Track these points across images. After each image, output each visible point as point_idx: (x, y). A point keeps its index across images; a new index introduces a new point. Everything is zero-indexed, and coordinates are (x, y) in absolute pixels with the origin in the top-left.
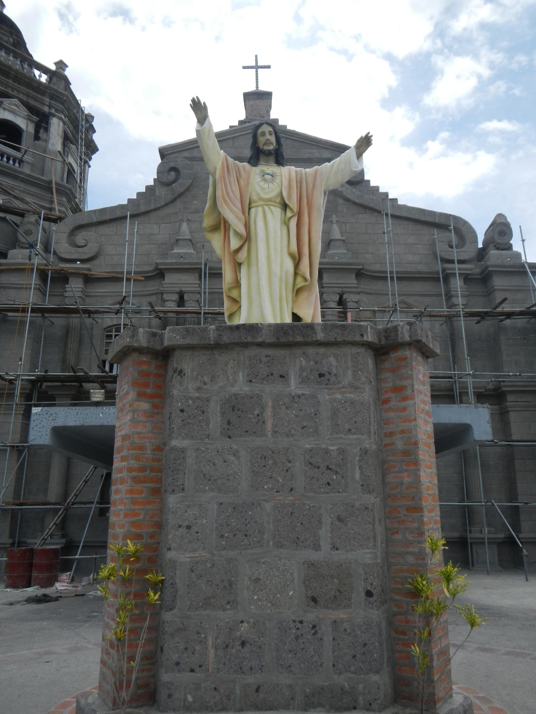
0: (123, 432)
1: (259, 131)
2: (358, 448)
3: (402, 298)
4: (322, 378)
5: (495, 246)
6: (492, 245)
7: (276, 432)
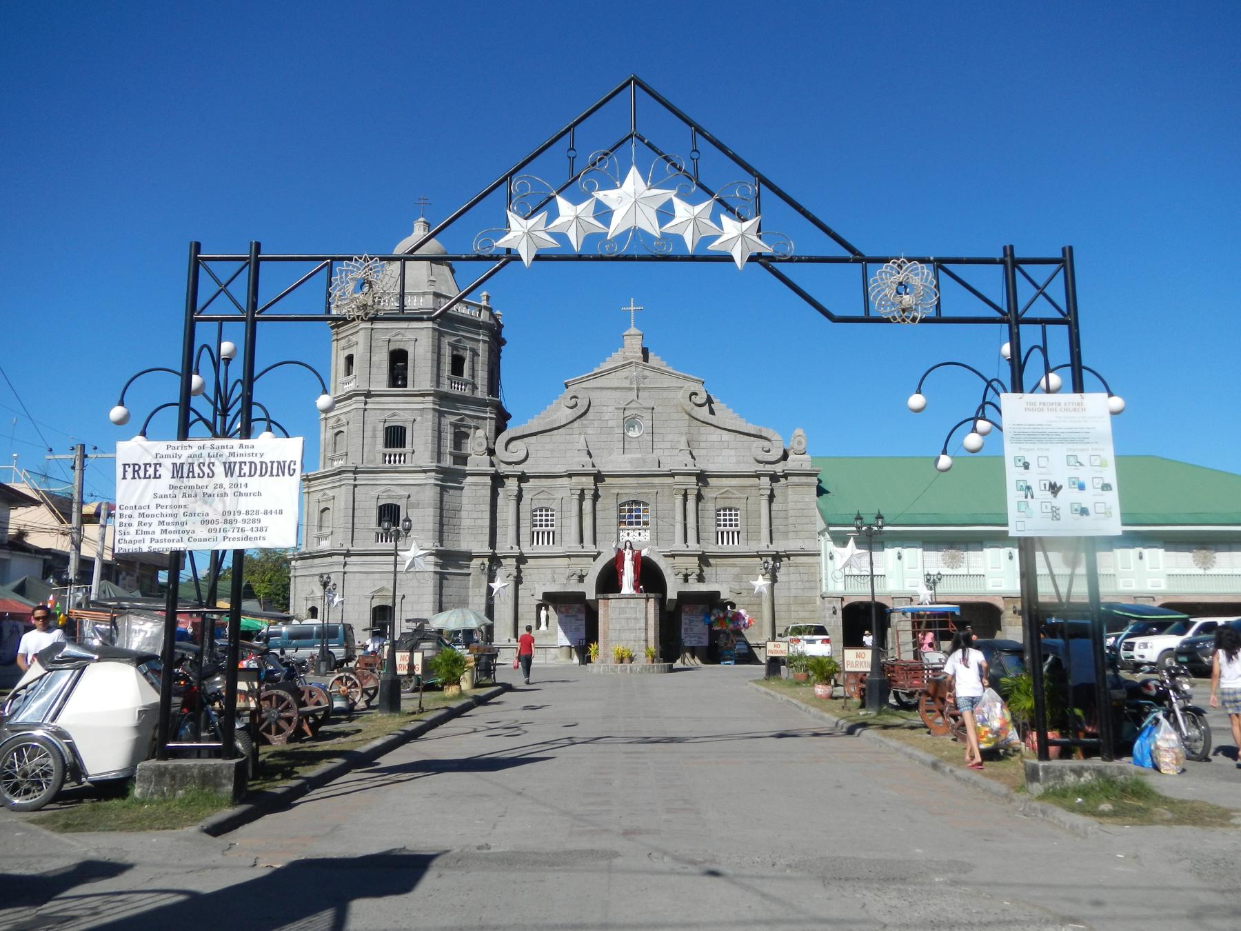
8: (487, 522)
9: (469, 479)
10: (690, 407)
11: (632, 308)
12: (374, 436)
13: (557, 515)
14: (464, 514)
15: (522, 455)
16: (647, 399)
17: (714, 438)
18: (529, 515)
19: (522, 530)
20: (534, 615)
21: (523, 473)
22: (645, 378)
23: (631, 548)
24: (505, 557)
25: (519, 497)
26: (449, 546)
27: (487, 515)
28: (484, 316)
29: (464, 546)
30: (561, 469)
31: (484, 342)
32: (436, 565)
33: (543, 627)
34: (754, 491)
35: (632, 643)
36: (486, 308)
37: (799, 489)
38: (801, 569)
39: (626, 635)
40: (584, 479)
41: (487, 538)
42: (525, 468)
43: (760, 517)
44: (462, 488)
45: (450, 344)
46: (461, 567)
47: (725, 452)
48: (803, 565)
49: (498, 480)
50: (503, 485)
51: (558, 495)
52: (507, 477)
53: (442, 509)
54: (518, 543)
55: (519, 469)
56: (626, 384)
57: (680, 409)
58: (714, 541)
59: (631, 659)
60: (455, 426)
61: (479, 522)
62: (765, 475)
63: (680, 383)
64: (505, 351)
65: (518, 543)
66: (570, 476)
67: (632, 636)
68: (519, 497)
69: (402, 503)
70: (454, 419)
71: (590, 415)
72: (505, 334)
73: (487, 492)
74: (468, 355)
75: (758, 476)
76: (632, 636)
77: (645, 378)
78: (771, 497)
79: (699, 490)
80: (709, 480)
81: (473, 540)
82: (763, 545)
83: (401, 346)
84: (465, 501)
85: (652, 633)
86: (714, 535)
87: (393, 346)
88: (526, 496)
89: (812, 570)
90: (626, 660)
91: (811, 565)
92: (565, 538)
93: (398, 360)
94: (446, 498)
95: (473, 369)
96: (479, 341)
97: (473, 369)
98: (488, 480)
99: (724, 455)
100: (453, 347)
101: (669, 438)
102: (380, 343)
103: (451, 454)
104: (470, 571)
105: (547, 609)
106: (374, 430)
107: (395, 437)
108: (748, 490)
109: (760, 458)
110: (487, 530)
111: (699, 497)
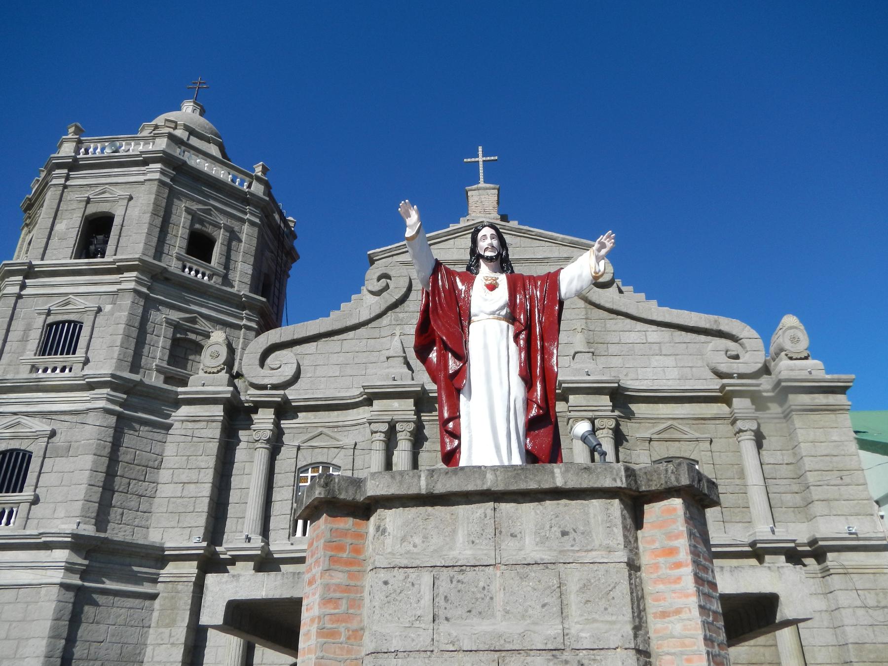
1: (480, 234)
2: (619, 636)
3: (670, 423)
4: (566, 537)
5: (786, 355)
6: (783, 353)
7: (507, 612)
8: (206, 490)
9: (185, 411)
11: (481, 159)
12: (24, 340)
14: (164, 475)
15: (288, 372)
17: (633, 337)
21: (286, 401)
23: (502, 262)
25: (275, 444)
26: (117, 533)
28: (257, 189)
29: (154, 537)
30: (354, 392)
31: (252, 224)
32: (70, 568)
34: (724, 429)
36: (258, 179)
38: (859, 581)
40: (395, 404)
41: (201, 520)
42: (292, 394)
43: (742, 474)
44: (168, 427)
45: (188, 211)
47: (656, 361)
48: (861, 570)
49: (237, 415)
50: (248, 424)
51: (347, 440)
52: (256, 407)
53: (113, 459)
54: (265, 532)
55: (276, 396)
60: (176, 327)
61: (191, 489)
62: (740, 394)
65: (265, 532)
66: (369, 400)
68: (275, 444)
69: (36, 448)
70: (175, 316)
72: (297, 244)
74: (221, 237)
75: (725, 398)
79: (618, 425)
80: (634, 407)
81: (172, 520)
82: (762, 530)
83: (103, 208)
84: (170, 450)
87: (92, 209)
93: (96, 231)
94: (129, 439)
95: (228, 257)
96: (243, 221)
97: (228, 257)
98: (218, 411)
102: (75, 205)
103: (159, 370)
106: (28, 329)
107: (60, 337)
108: (711, 426)
110: (204, 505)
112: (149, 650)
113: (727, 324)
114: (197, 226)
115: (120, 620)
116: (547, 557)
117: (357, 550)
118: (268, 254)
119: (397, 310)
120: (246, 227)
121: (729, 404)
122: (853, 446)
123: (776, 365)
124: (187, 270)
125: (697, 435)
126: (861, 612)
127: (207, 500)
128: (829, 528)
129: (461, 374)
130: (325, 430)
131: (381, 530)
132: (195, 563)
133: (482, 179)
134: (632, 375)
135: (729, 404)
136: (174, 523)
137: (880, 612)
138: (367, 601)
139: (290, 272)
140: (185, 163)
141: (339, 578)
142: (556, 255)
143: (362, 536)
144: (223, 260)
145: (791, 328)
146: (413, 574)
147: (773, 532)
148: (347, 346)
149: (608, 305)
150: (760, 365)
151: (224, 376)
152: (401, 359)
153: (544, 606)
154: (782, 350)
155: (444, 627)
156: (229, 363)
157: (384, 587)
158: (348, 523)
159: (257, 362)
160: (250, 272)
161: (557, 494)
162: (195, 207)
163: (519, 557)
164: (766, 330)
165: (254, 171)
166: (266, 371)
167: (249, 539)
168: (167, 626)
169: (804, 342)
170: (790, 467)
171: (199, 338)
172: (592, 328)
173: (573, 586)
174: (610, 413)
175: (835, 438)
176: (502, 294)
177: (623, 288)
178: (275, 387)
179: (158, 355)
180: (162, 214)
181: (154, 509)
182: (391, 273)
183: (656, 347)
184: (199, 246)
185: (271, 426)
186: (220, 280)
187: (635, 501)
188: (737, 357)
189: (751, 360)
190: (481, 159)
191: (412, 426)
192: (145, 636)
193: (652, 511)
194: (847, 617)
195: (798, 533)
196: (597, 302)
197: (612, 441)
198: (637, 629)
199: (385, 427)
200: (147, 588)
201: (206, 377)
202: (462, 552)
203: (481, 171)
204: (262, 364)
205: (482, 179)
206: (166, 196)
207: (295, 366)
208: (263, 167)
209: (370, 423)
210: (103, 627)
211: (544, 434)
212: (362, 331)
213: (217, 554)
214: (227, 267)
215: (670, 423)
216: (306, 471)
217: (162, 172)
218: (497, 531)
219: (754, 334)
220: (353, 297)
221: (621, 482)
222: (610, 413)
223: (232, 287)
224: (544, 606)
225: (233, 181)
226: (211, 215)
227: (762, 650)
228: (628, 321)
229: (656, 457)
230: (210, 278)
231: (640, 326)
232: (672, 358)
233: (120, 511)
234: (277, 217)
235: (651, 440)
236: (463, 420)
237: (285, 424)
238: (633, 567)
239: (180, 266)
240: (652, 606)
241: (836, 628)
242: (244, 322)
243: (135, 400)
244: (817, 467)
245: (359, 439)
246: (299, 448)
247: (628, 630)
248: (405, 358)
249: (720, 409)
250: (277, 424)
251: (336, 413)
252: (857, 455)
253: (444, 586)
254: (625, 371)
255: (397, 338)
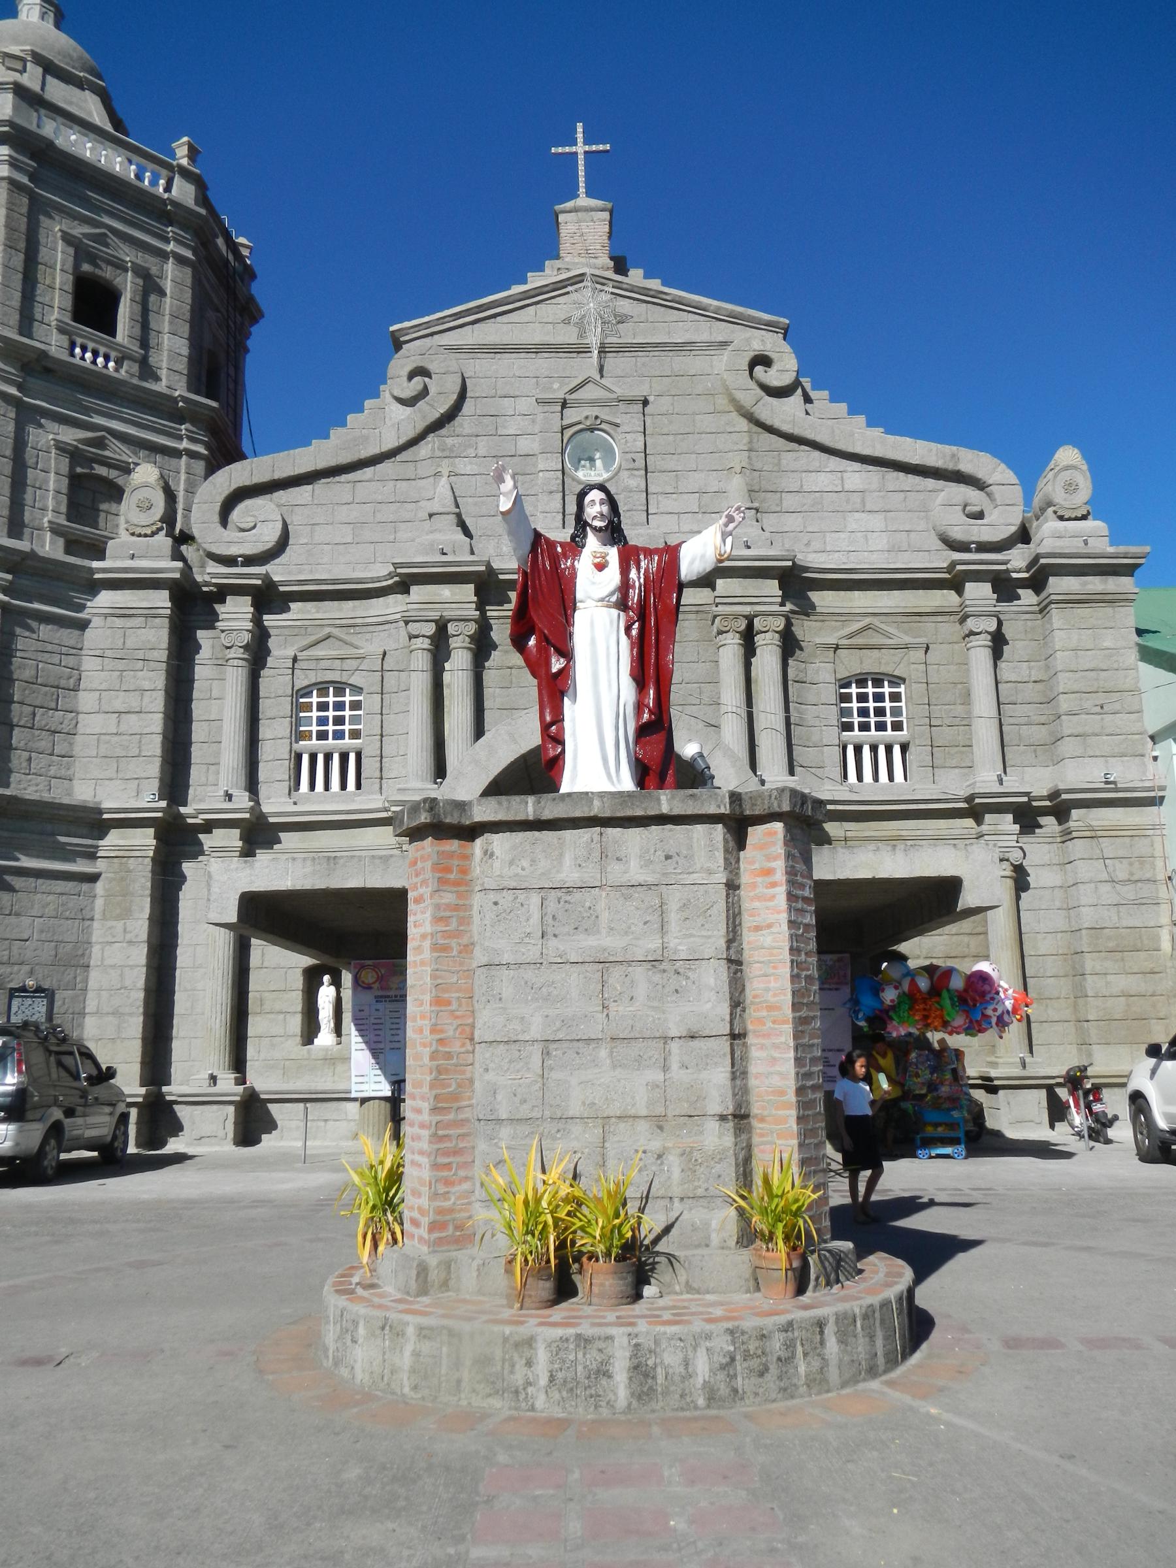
0: (421, 930)
1: (588, 499)
5: (1055, 512)
6: (1051, 509)
8: (155, 723)
9: (106, 599)
10: (750, 395)
11: (580, 148)
13: (371, 702)
14: (86, 700)
15: (268, 536)
16: (625, 375)
17: (822, 481)
18: (286, 706)
19: (266, 751)
20: (296, 1000)
22: (622, 319)
23: (613, 532)
24: (208, 827)
27: (156, 702)
28: (183, 192)
29: (82, 793)
30: (379, 571)
31: (181, 260)
33: (325, 1038)
34: (950, 629)
35: (644, 1138)
36: (185, 173)
37: (1082, 612)
38: (1108, 847)
39: (588, 1084)
40: (446, 592)
41: (154, 769)
42: (278, 571)
43: (966, 697)
44: (83, 625)
45: (68, 239)
46: (68, 854)
47: (856, 521)
48: (1114, 833)
49: (192, 607)
50: (211, 621)
52: (222, 593)
54: (252, 785)
55: (253, 575)
56: (569, 336)
57: (722, 402)
58: (836, 773)
59: (638, 1263)
60: (74, 455)
62: (977, 576)
63: (721, 331)
64: (261, 342)
65: (252, 785)
66: (403, 585)
67: (637, 1088)
68: (258, 653)
70: (71, 436)
71: (463, 423)
72: (259, 290)
73: (158, 636)
74: (128, 286)
75: (956, 583)
76: (637, 1088)
77: (622, 319)
78: (998, 642)
79: (789, 624)
80: (815, 596)
82: (986, 779)
84: (89, 664)
85: (776, 1068)
86: (837, 751)
88: (280, 651)
89: (1141, 847)
90: (600, 1279)
91: (1137, 833)
92: (393, 768)
95: (145, 326)
96: (163, 255)
97: (145, 326)
98: (161, 599)
99: (861, 521)
100: (80, 251)
101: (695, 481)
103: (56, 530)
104: (100, 866)
105: (336, 983)
108: (929, 625)
109: (957, 534)
110: (154, 746)
111: (789, 645)
112: (96, 950)
113: (971, 461)
114: (86, 267)
115: (50, 910)
116: (650, 879)
117: (464, 871)
118: (211, 315)
119: (443, 432)
120: (170, 266)
121: (960, 591)
122: (1132, 656)
123: (1039, 527)
124: (78, 350)
125: (907, 639)
126: (1106, 888)
127: (158, 739)
128: (1079, 774)
129: (565, 673)
130: (336, 631)
131: (488, 854)
132: (151, 831)
133: (582, 190)
134: (816, 545)
135: (960, 591)
136: (111, 773)
137: (1131, 887)
138: (476, 919)
139: (250, 343)
140: (50, 144)
141: (448, 898)
142: (705, 337)
143: (467, 857)
144: (137, 331)
145: (1067, 468)
146: (522, 896)
147: (1001, 782)
148: (363, 491)
149: (786, 428)
150: (1013, 529)
151: (163, 541)
152: (453, 518)
153: (645, 923)
154: (1050, 504)
155: (552, 943)
156: (169, 519)
157: (495, 908)
158: (453, 845)
159: (216, 518)
160: (185, 351)
161: (663, 820)
162: (79, 230)
163: (624, 880)
164: (1030, 470)
165: (172, 154)
166: (230, 534)
167: (229, 797)
168: (118, 918)
169: (1085, 491)
170: (1039, 686)
171: (113, 474)
172: (758, 466)
173: (673, 906)
174: (777, 608)
175: (1106, 644)
176: (612, 577)
177: (813, 394)
178: (250, 561)
179: (50, 504)
180: (22, 245)
181: (77, 750)
182: (431, 367)
183: (856, 498)
184: (94, 305)
185: (250, 626)
186: (135, 368)
187: (738, 824)
188: (980, 515)
189: (1000, 523)
190: (580, 148)
191: (472, 628)
192: (88, 931)
193: (756, 834)
194: (1085, 895)
195: (1033, 781)
196: (769, 422)
197: (778, 651)
198: (730, 942)
199: (430, 629)
200: (81, 866)
201: (133, 541)
202: (569, 874)
203: (582, 179)
204: (224, 522)
205: (582, 190)
206: (24, 210)
207: (279, 525)
208: (192, 148)
209: (407, 623)
210: (25, 921)
211: (657, 738)
212: (385, 467)
213: (182, 817)
214: (144, 343)
215: (868, 620)
216: (309, 694)
217: (13, 164)
218: (603, 855)
219: (1010, 476)
220: (368, 403)
221: (725, 809)
222: (777, 608)
223: (157, 379)
224: (645, 923)
225: (139, 177)
226: (107, 245)
227: (966, 939)
228: (817, 454)
229: (843, 673)
230: (119, 363)
231: (834, 462)
232: (881, 516)
233: (26, 755)
234: (220, 241)
235: (837, 648)
236: (567, 724)
237: (269, 620)
238: (732, 886)
239: (66, 344)
240: (747, 921)
241: (1070, 909)
242: (185, 444)
243: (25, 582)
244: (1076, 687)
245: (390, 645)
246: (295, 660)
247: (722, 943)
248: (459, 515)
249: (946, 598)
250: (257, 621)
251: (350, 603)
252: (1136, 669)
253: (552, 906)
254: (805, 538)
255: (444, 481)
